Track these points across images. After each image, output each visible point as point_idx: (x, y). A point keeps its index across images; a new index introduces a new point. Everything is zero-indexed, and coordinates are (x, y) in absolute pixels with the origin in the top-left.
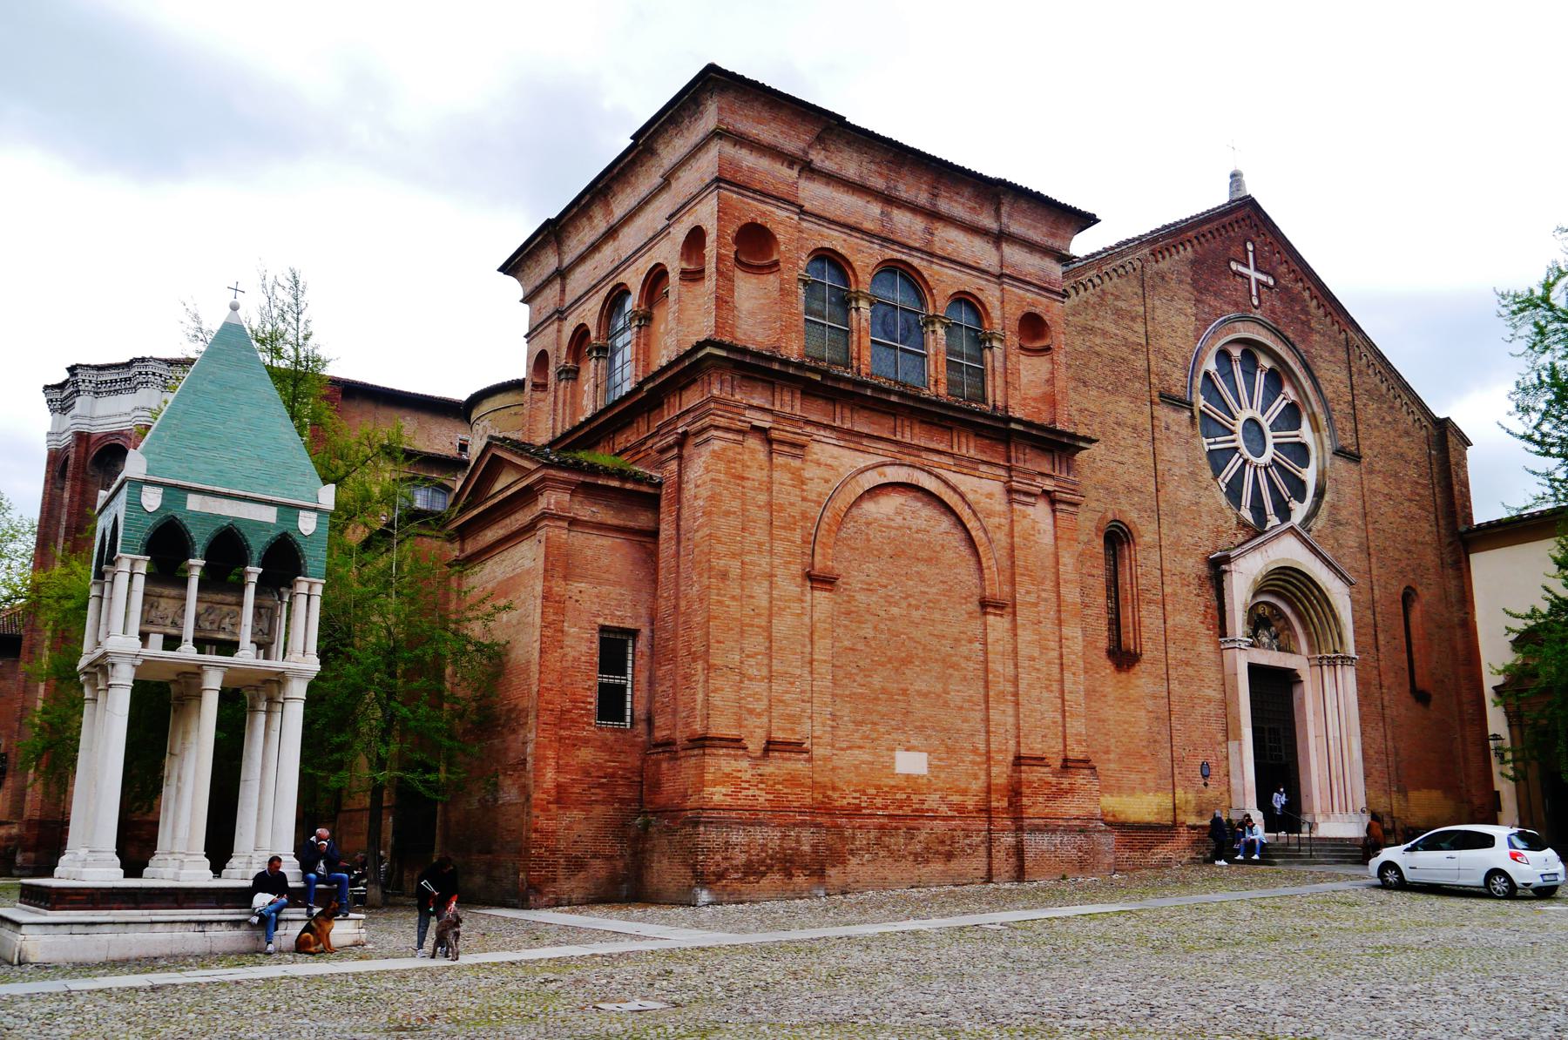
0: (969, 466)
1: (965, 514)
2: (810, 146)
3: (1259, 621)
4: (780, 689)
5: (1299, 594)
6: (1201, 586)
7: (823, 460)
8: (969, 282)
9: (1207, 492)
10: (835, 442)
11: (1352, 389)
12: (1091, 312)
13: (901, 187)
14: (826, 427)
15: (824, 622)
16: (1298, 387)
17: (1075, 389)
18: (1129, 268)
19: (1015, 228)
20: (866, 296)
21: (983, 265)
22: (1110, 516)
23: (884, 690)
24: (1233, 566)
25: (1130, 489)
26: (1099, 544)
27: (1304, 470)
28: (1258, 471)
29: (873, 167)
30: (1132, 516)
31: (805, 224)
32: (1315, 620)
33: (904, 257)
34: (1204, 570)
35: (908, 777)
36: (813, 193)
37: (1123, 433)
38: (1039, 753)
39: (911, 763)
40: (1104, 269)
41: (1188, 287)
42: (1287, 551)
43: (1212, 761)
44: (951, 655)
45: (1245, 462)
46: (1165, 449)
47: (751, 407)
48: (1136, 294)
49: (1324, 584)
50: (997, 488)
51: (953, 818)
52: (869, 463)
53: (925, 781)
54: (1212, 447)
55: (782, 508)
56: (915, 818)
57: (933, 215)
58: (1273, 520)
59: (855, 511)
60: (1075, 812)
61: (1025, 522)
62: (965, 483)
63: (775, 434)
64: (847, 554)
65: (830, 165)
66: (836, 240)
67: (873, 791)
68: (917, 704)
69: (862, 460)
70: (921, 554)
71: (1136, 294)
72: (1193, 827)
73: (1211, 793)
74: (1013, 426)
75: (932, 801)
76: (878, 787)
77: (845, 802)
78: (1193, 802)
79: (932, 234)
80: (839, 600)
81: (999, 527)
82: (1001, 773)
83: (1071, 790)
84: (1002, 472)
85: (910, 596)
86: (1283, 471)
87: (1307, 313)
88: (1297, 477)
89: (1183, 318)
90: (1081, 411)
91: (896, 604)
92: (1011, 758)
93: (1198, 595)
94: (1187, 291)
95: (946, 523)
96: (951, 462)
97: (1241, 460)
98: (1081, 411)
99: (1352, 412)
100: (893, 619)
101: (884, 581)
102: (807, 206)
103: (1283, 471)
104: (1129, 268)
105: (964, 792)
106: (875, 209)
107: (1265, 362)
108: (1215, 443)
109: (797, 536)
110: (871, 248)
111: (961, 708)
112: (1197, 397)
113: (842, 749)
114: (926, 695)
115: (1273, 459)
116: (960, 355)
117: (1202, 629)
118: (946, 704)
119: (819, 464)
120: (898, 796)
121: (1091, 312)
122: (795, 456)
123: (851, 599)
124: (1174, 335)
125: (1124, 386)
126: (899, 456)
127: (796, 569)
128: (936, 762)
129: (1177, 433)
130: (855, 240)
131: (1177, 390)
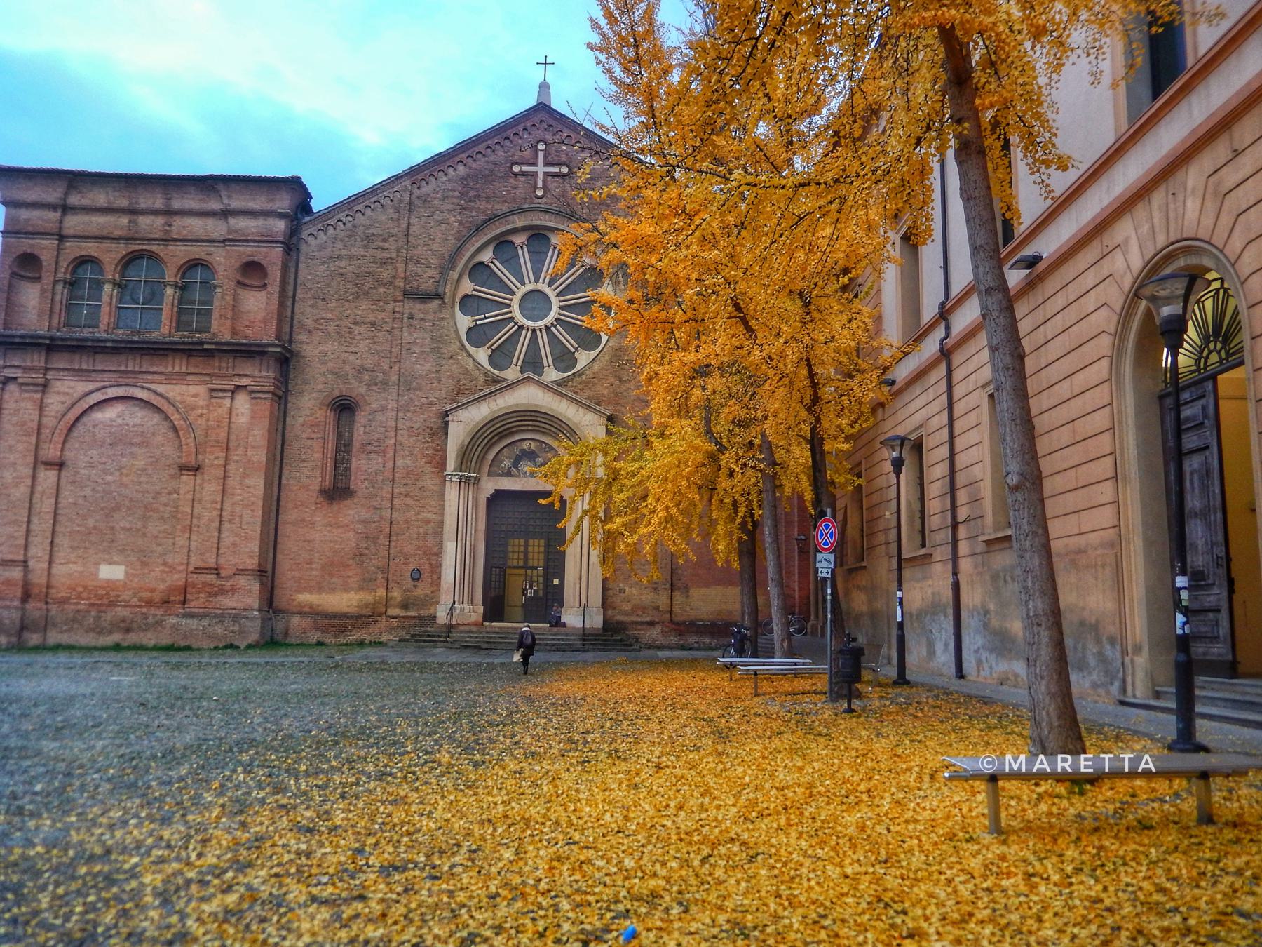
0: (181, 378)
1: (170, 410)
2: (66, 194)
6: (431, 435)
8: (197, 251)
12: (339, 245)
13: (141, 200)
14: (64, 370)
17: (313, 306)
19: (236, 204)
20: (109, 281)
21: (215, 235)
22: (337, 393)
23: (95, 528)
24: (450, 418)
25: (361, 370)
26: (324, 416)
29: (117, 194)
30: (357, 389)
34: (436, 422)
35: (108, 581)
36: (74, 223)
37: (357, 329)
38: (214, 566)
39: (111, 572)
40: (355, 209)
41: (456, 201)
43: (426, 568)
46: (406, 334)
47: (5, 367)
48: (392, 219)
50: (202, 390)
51: (140, 606)
55: (24, 424)
56: (109, 606)
57: (169, 213)
59: (85, 419)
60: (234, 605)
61: (220, 411)
62: (173, 391)
63: (20, 380)
65: (85, 202)
66: (91, 248)
68: (121, 536)
69: (91, 386)
70: (135, 440)
71: (392, 219)
72: (395, 618)
73: (422, 589)
74: (206, 346)
75: (126, 596)
76: (85, 587)
78: (399, 599)
79: (170, 226)
81: (201, 416)
82: (178, 579)
83: (233, 590)
84: (208, 379)
86: (572, 328)
90: (316, 321)
91: (112, 474)
92: (191, 569)
95: (157, 418)
96: (163, 377)
98: (316, 321)
100: (108, 483)
101: (104, 460)
102: (71, 232)
103: (572, 328)
105: (153, 590)
106: (124, 220)
109: (33, 439)
111: (156, 537)
116: (193, 303)
117: (428, 468)
118: (144, 535)
119: (59, 393)
122: (36, 392)
123: (77, 473)
125: (366, 294)
127: (30, 459)
130: (107, 245)
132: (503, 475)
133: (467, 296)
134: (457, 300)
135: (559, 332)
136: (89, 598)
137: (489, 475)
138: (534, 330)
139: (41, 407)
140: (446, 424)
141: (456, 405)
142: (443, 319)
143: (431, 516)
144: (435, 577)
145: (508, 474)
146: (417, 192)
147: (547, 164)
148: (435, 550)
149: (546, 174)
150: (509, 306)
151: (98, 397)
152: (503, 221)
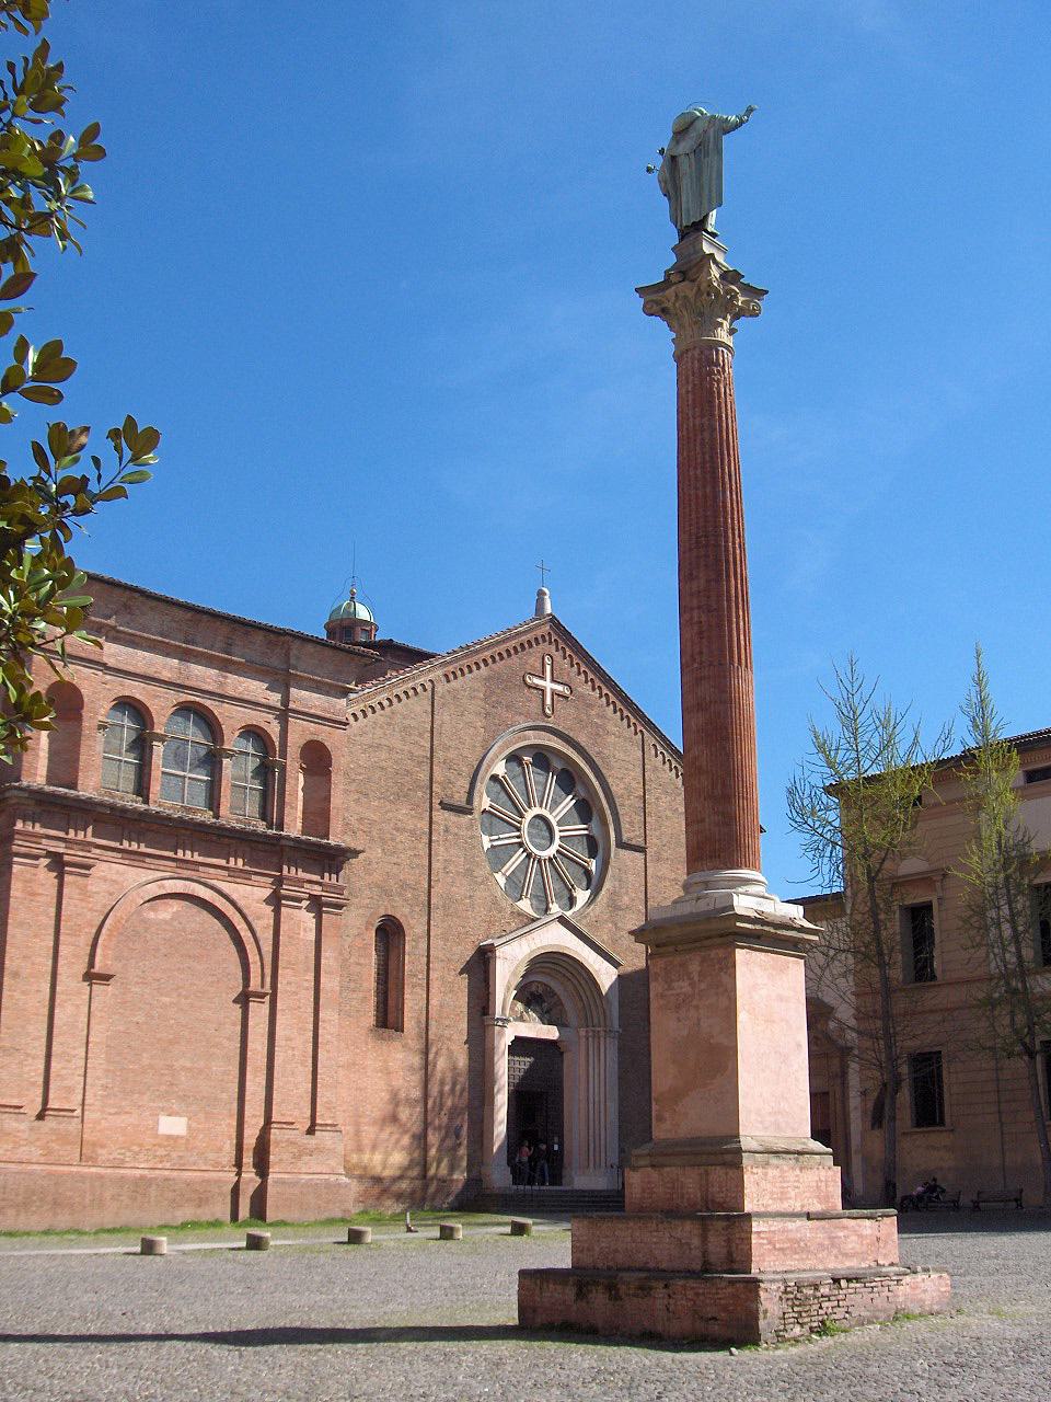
3: (532, 995)
4: (59, 1066)
5: (568, 975)
7: (109, 876)
10: (121, 861)
15: (101, 1011)
18: (419, 689)
23: (151, 1066)
25: (404, 886)
30: (402, 913)
31: (108, 677)
33: (198, 699)
35: (169, 1137)
37: (400, 837)
42: (554, 937)
44: (215, 1037)
45: (529, 856)
49: (591, 965)
52: (150, 877)
53: (184, 1141)
54: (495, 843)
58: (555, 909)
62: (236, 890)
64: (125, 954)
66: (136, 690)
67: (136, 1148)
76: (140, 1145)
77: (111, 1157)
80: (117, 993)
83: (319, 1150)
85: (179, 988)
87: (603, 717)
96: (226, 873)
97: (525, 854)
101: (158, 975)
104: (419, 689)
108: (499, 839)
110: (167, 693)
112: (481, 798)
113: (110, 1114)
114: (190, 1070)
115: (558, 851)
120: (158, 1153)
121: (379, 732)
124: (460, 746)
126: (179, 871)
128: (194, 1125)
131: (460, 798)
136: (147, 1161)
139: (85, 894)
147: (553, 681)
149: (554, 693)
151: (154, 890)
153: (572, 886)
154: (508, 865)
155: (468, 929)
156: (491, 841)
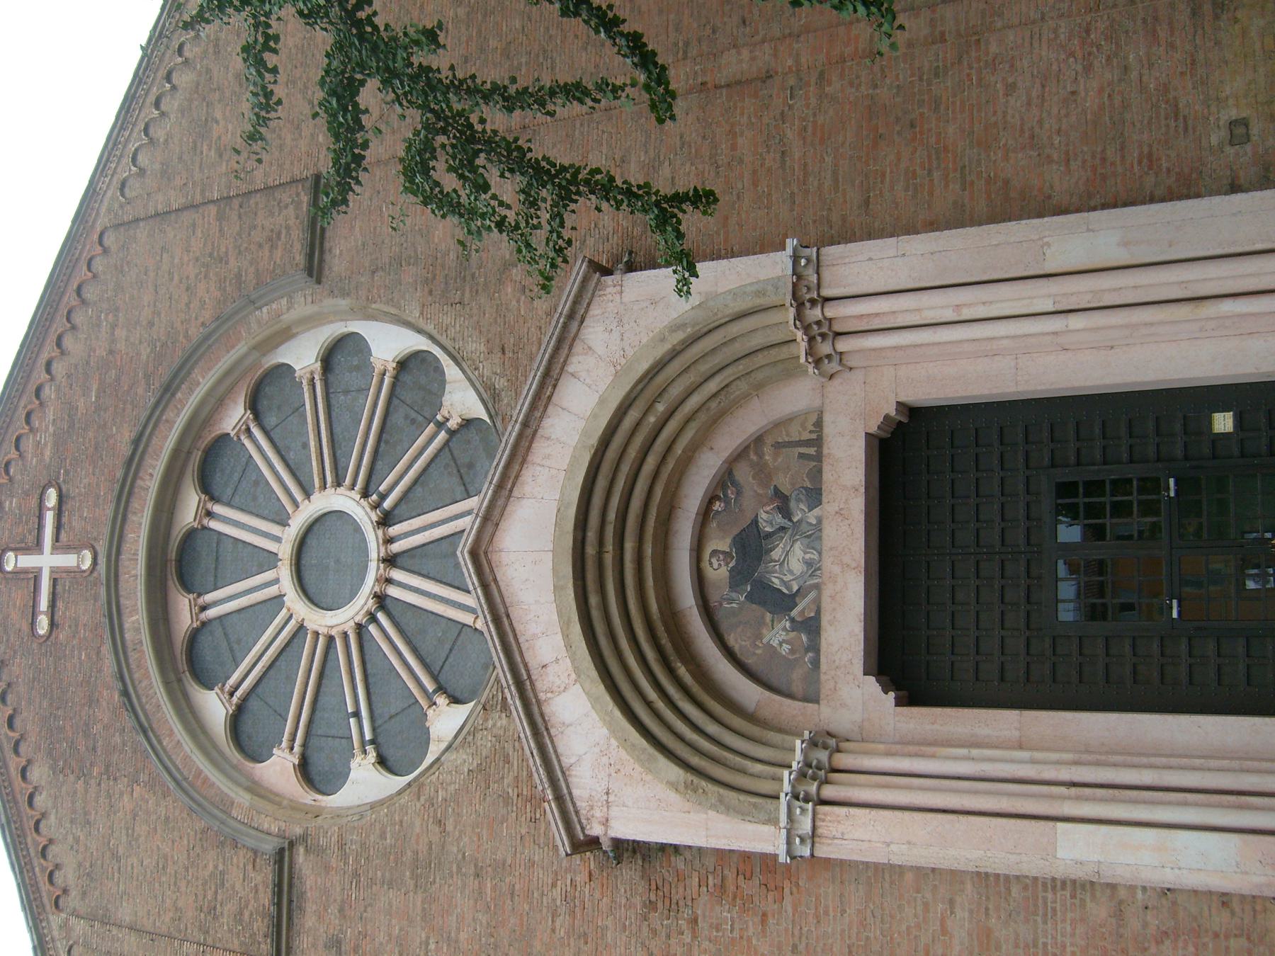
6: (673, 908)
9: (450, 828)
11: (192, 206)
16: (215, 403)
24: (596, 830)
27: (378, 367)
28: (396, 547)
32: (712, 386)
49: (602, 401)
54: (368, 736)
88: (396, 378)
89: (142, 829)
93: (694, 921)
94: (98, 797)
97: (381, 616)
99: (236, 202)
107: (190, 504)
108: (357, 714)
129: (341, 910)
132: (814, 647)
133: (304, 769)
134: (308, 797)
135: (396, 483)
137: (812, 698)
138: (391, 561)
140: (625, 850)
141: (551, 809)
142: (342, 845)
143: (961, 926)
144: (1220, 920)
145: (812, 627)
146: (73, 901)
147: (37, 547)
148: (1099, 911)
149: (58, 546)
150: (331, 639)
152: (133, 657)
153: (440, 425)
154: (411, 685)
155: (557, 893)
156: (363, 743)
